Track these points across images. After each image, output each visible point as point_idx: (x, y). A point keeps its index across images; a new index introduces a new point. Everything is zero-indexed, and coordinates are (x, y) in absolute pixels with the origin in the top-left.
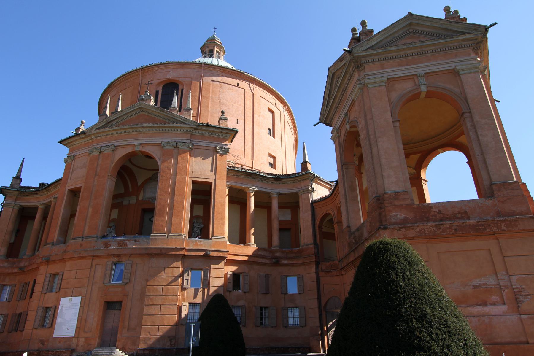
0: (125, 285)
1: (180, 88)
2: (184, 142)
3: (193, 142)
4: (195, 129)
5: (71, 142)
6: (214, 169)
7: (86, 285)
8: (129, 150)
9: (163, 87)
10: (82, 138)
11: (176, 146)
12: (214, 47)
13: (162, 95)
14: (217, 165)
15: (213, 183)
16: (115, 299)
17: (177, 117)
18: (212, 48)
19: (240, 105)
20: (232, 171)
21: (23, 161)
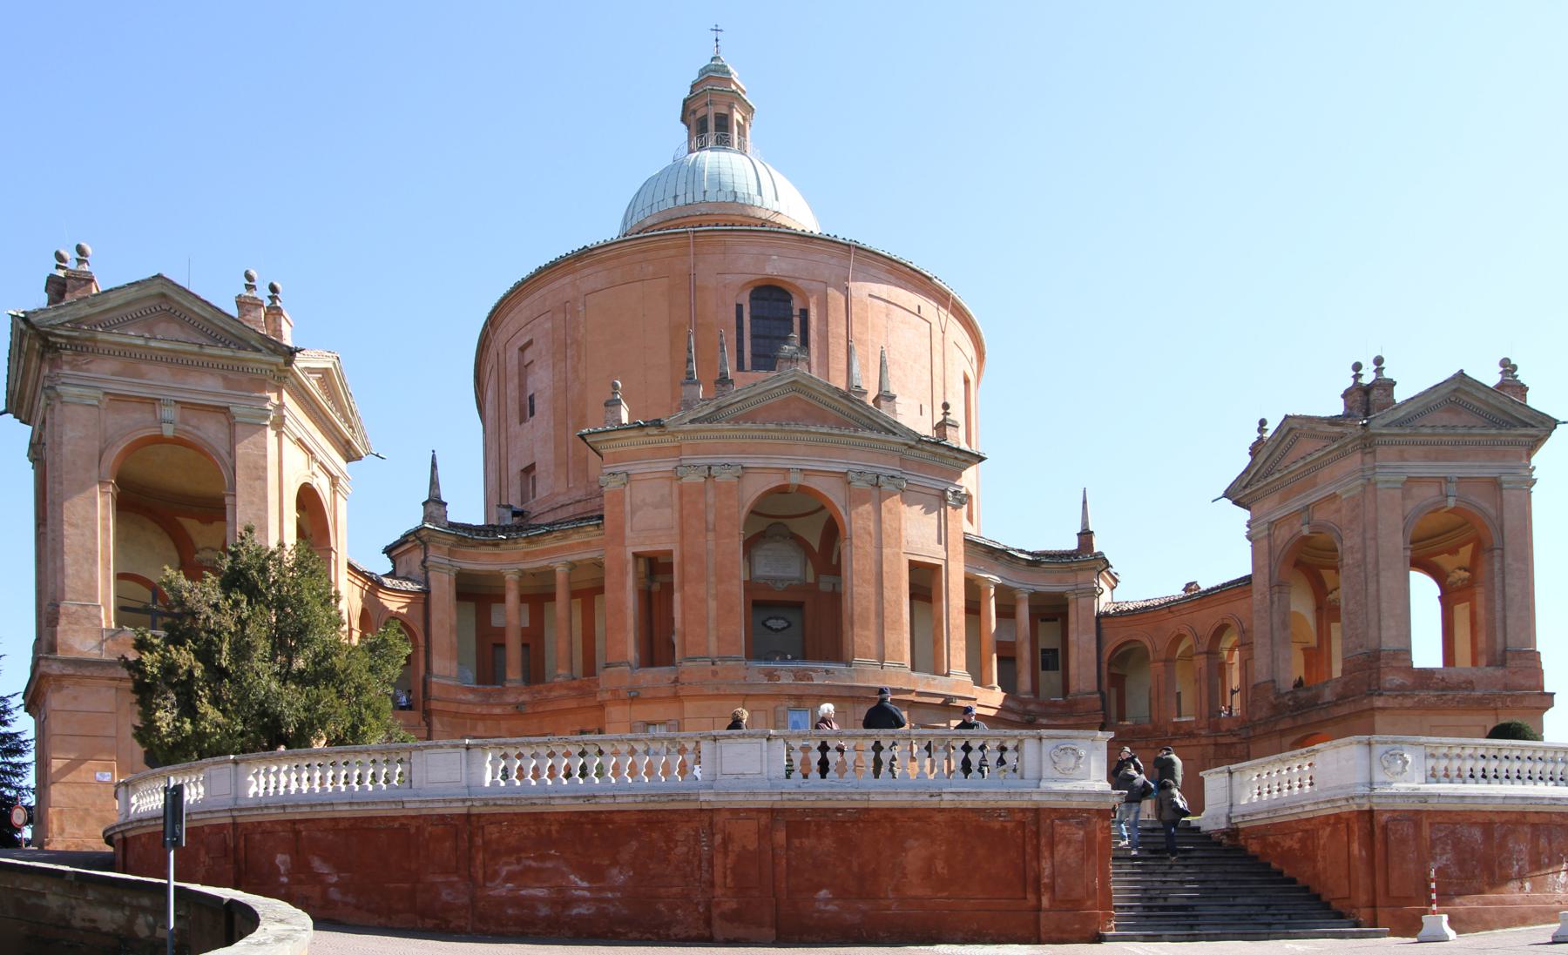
1: (796, 305)
2: (892, 477)
3: (907, 477)
4: (911, 447)
5: (607, 440)
8: (775, 481)
9: (751, 295)
10: (648, 435)
11: (877, 484)
12: (731, 107)
13: (753, 317)
17: (877, 417)
18: (724, 111)
19: (924, 368)
20: (971, 545)
21: (434, 457)
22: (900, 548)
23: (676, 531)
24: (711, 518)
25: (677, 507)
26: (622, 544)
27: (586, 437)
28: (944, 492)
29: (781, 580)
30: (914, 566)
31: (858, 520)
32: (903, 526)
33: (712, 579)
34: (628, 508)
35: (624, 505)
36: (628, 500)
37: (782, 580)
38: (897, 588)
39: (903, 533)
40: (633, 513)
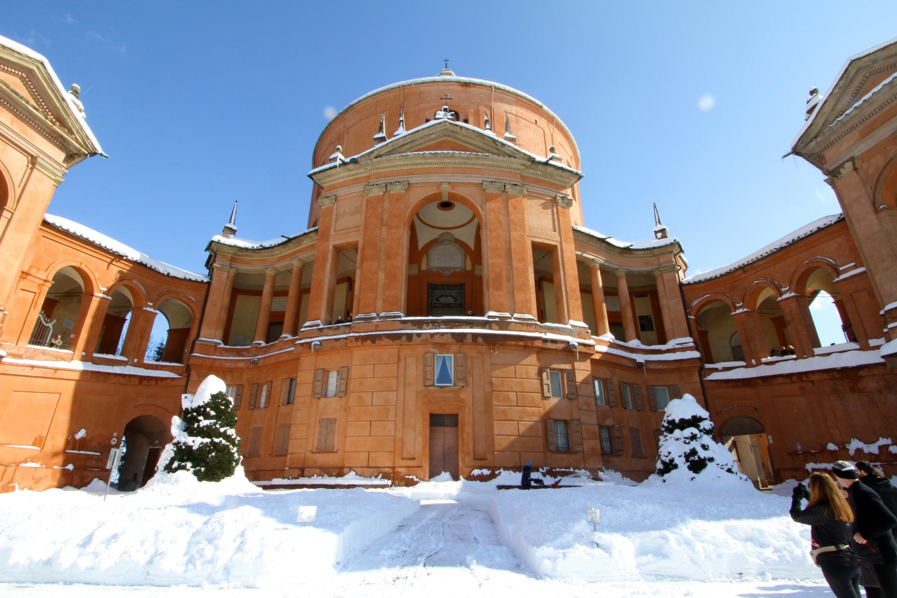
0: (460, 389)
6: (557, 226)
7: (394, 388)
10: (350, 170)
14: (561, 223)
15: (559, 247)
16: (447, 410)
22: (524, 232)
23: (362, 227)
24: (385, 217)
25: (364, 213)
26: (327, 240)
27: (313, 177)
28: (555, 198)
29: (448, 269)
30: (536, 247)
31: (491, 212)
32: (526, 218)
33: (383, 258)
34: (334, 217)
35: (332, 216)
36: (334, 212)
37: (448, 269)
38: (522, 260)
39: (527, 223)
40: (337, 220)
